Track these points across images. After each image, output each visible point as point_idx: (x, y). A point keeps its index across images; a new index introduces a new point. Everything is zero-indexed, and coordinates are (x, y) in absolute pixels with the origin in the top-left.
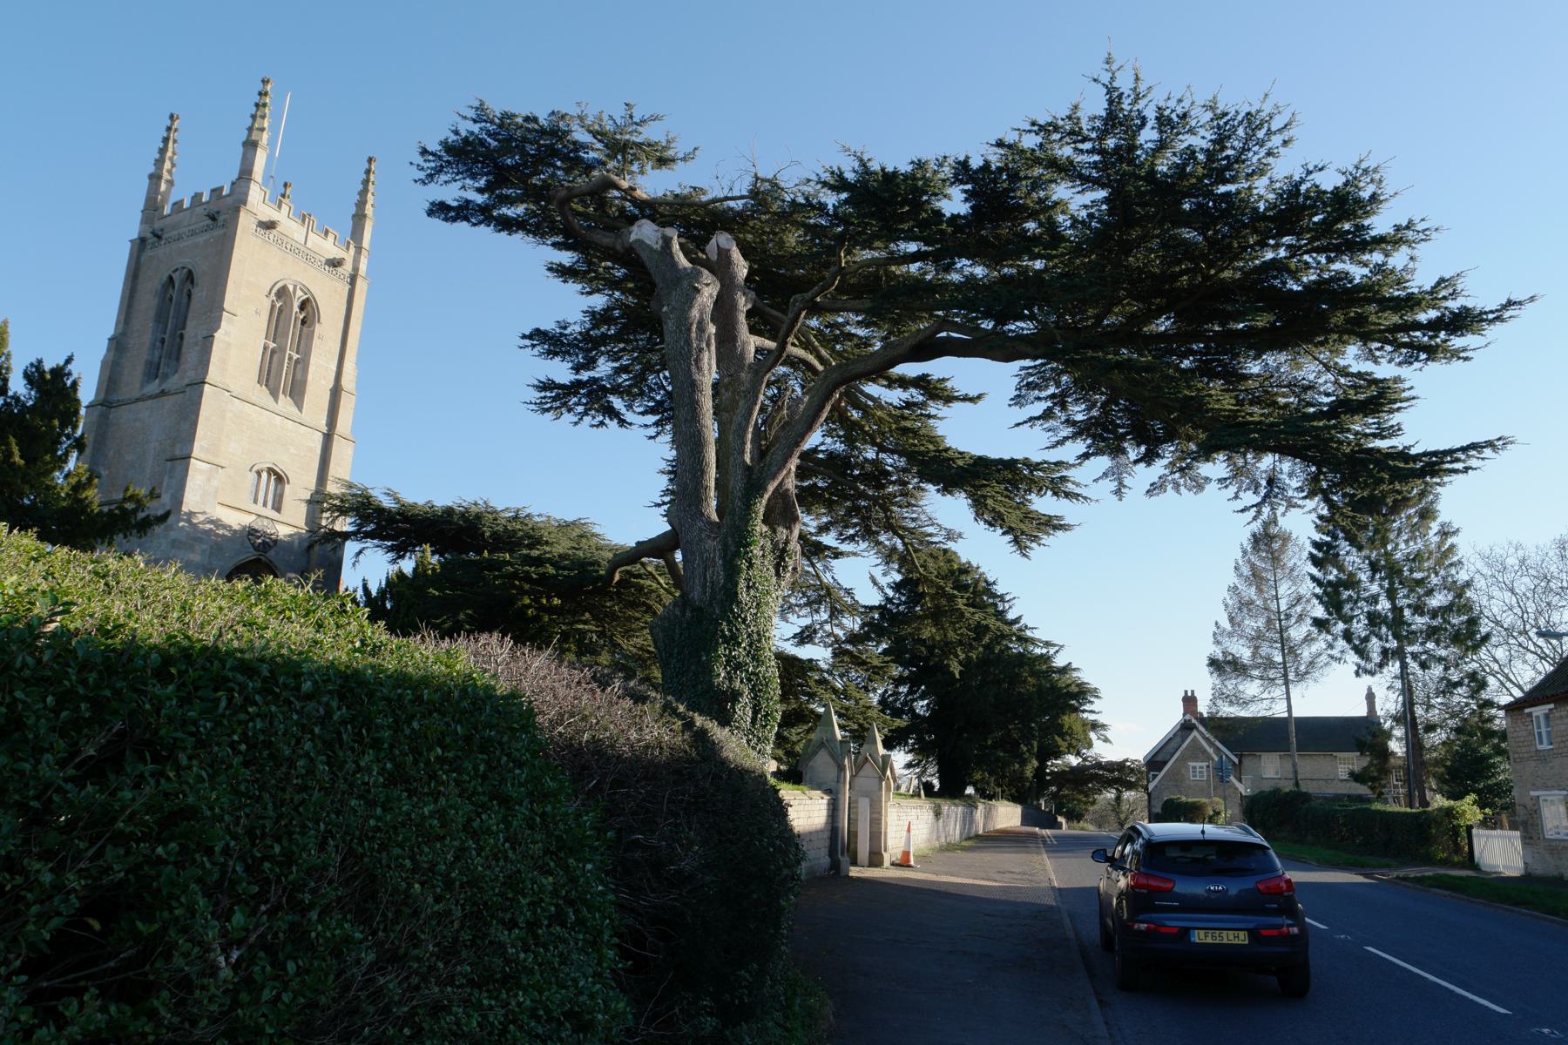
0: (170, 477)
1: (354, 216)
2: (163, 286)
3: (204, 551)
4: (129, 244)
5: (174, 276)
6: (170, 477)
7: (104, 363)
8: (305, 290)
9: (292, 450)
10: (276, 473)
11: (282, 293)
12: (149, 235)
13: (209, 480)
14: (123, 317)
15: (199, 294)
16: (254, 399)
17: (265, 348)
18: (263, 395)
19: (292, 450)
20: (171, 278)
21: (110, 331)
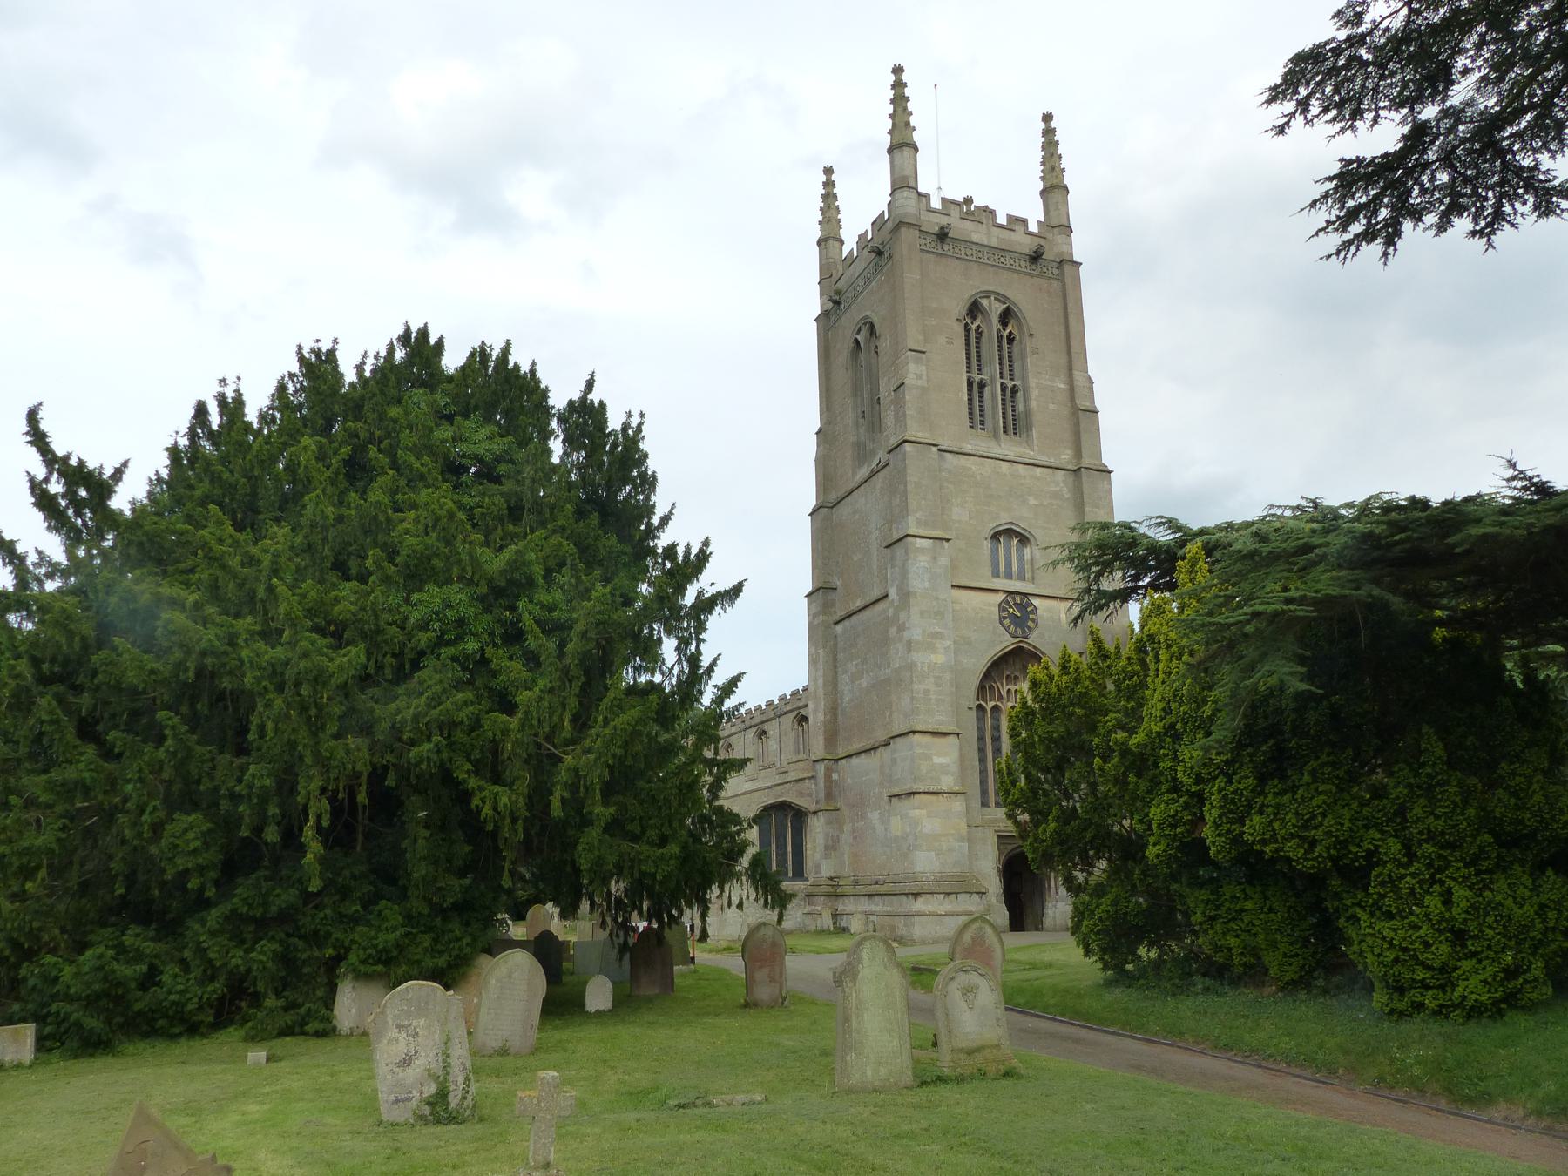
0: (893, 567)
1: (1043, 193)
2: (853, 351)
3: (947, 649)
4: (815, 323)
5: (858, 337)
6: (893, 567)
7: (817, 460)
8: (1000, 298)
9: (1032, 501)
10: (1018, 534)
11: (974, 309)
12: (830, 305)
13: (934, 558)
14: (824, 406)
15: (885, 344)
16: (969, 448)
17: (970, 384)
18: (977, 442)
19: (1032, 501)
20: (857, 342)
21: (816, 424)
